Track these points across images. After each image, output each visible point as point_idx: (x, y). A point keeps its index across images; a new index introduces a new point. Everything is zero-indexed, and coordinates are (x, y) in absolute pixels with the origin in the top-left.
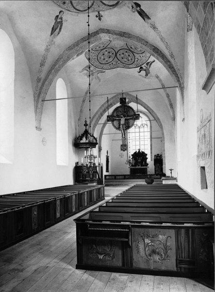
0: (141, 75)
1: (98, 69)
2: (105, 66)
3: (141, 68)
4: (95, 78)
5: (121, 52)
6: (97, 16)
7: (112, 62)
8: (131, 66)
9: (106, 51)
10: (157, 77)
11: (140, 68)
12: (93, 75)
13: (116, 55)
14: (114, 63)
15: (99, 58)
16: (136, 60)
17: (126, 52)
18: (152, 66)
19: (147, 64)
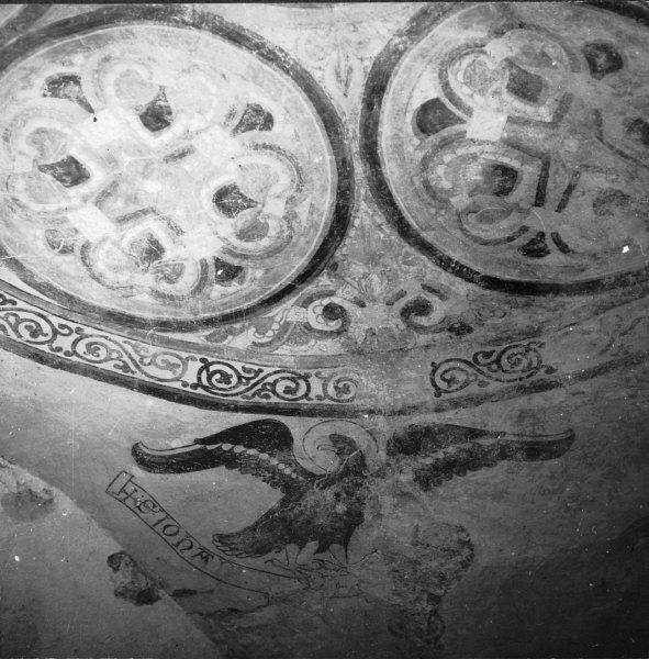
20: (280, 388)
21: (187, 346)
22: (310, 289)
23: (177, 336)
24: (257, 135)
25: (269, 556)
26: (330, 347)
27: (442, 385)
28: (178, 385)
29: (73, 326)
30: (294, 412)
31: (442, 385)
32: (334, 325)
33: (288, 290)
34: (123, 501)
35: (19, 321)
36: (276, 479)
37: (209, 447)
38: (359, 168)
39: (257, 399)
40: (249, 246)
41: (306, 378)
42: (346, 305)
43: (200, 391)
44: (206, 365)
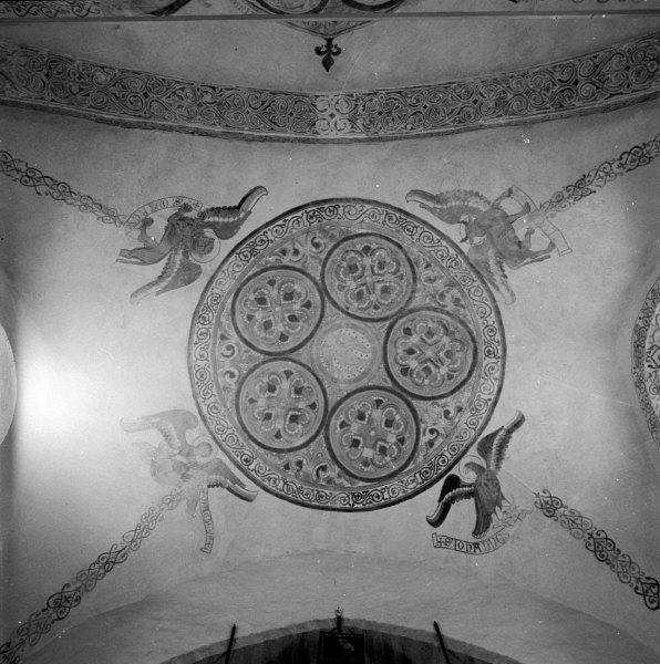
3: (453, 482)
4: (191, 506)
5: (355, 404)
6: (318, 51)
7: (300, 455)
8: (396, 488)
9: (288, 374)
10: (550, 507)
11: (445, 490)
13: (325, 424)
14: (309, 469)
15: (243, 399)
16: (424, 439)
17: (379, 402)
18: (508, 452)
19: (484, 449)
24: (381, 406)
26: (441, 440)
30: (451, 468)
32: (435, 434)
36: (468, 495)
40: (401, 430)
41: (443, 454)
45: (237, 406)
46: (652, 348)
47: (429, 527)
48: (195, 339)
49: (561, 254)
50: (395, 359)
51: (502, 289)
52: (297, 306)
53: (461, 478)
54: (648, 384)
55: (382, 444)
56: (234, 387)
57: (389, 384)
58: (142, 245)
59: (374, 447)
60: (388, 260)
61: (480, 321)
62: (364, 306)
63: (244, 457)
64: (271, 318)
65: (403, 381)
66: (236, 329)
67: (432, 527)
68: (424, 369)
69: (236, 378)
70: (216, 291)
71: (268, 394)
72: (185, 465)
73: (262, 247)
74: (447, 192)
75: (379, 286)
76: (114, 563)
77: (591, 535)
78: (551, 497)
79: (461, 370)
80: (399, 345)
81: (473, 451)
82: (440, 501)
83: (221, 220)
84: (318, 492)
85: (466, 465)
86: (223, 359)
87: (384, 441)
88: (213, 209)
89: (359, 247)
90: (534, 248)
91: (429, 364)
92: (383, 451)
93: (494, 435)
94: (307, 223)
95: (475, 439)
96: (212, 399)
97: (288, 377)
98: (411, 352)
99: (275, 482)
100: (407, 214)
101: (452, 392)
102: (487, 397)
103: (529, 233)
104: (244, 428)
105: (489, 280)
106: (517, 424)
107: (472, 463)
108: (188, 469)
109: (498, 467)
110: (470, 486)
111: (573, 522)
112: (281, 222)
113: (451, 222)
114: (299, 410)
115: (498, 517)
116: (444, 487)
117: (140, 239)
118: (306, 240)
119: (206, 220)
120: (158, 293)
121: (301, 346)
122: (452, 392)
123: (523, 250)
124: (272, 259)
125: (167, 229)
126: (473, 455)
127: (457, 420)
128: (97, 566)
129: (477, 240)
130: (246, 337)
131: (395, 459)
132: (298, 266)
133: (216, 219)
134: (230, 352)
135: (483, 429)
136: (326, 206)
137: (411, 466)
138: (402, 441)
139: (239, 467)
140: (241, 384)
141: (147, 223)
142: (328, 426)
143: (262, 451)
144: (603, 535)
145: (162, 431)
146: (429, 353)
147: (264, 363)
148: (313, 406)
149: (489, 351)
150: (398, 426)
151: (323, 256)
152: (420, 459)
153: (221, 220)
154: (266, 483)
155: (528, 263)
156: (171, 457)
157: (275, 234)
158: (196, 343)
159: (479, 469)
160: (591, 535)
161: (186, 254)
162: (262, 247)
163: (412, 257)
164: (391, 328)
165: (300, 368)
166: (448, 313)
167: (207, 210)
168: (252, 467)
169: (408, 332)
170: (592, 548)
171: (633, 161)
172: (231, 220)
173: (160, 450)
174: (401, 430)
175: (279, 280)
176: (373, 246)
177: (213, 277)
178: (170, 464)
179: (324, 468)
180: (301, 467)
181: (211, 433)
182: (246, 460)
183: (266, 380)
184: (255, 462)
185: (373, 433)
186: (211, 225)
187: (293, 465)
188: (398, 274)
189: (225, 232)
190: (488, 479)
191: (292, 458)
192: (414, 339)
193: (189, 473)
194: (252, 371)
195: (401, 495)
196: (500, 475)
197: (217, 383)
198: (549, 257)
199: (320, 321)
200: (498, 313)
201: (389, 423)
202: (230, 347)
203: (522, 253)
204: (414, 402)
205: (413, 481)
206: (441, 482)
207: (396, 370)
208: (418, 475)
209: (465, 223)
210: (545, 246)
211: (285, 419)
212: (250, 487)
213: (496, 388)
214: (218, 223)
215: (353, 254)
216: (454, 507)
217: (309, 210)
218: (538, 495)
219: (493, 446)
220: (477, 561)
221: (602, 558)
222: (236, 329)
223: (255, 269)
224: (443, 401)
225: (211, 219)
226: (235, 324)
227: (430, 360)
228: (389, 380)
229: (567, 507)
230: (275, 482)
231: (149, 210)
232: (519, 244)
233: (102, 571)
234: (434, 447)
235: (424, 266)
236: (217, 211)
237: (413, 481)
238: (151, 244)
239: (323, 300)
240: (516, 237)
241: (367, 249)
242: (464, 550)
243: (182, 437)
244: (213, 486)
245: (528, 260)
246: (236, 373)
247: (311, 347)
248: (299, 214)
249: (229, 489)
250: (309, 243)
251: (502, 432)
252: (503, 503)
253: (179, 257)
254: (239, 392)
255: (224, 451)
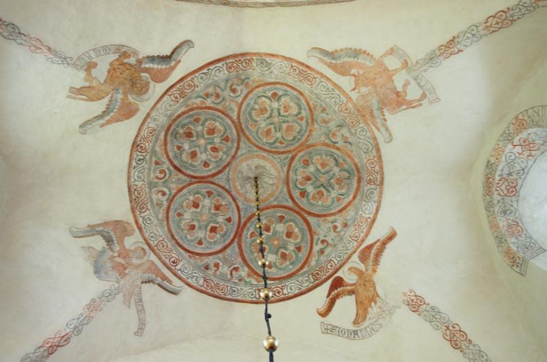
0: (330, 330)
1: (153, 257)
2: (185, 265)
3: (338, 283)
8: (292, 286)
10: (416, 304)
12: (122, 275)
13: (238, 234)
14: (225, 269)
16: (317, 248)
17: (282, 218)
19: (364, 257)
20: (329, 267)
21: (305, 272)
22: (315, 241)
23: (302, 272)
24: (284, 220)
25: (368, 317)
27: (356, 239)
28: (312, 284)
29: (283, 285)
31: (356, 239)
32: (325, 244)
33: (312, 244)
34: (327, 333)
35: (274, 292)
36: (351, 292)
37: (331, 297)
38: (297, 209)
39: (328, 274)
40: (298, 241)
42: (324, 239)
43: (316, 282)
44: (312, 274)
45: (167, 218)
46: (500, 180)
47: (321, 319)
48: (134, 164)
49: (431, 103)
50: (296, 185)
51: (382, 129)
52: (217, 140)
53: (345, 279)
54: (497, 209)
55: (283, 251)
56: (165, 204)
57: (290, 204)
58: (87, 84)
59: (276, 253)
60: (292, 104)
61: (363, 155)
62: (271, 141)
63: (172, 260)
64: (197, 149)
65: (303, 203)
66: (168, 156)
67: (320, 317)
68: (318, 193)
69: (166, 197)
70: (151, 125)
71: (193, 209)
72: (123, 265)
73: (189, 91)
74: (341, 50)
75: (284, 126)
76: (58, 346)
77: (448, 328)
78: (416, 296)
79: (347, 194)
80: (298, 172)
81: (355, 258)
82: (328, 296)
83: (156, 66)
84: (232, 287)
85: (350, 269)
86: (156, 180)
87: (286, 249)
88: (148, 57)
89: (269, 94)
90: (408, 98)
91: (322, 189)
92: (284, 256)
93: (370, 247)
94: (226, 72)
95: (358, 247)
96: (147, 213)
97: (209, 196)
98: (308, 179)
99: (197, 280)
100: (308, 67)
101: (340, 211)
102: (367, 216)
103: (406, 84)
104: (172, 236)
105: (372, 123)
106: (391, 237)
107: (356, 268)
108: (125, 269)
109: (374, 271)
110: (352, 285)
111: (433, 315)
112: (205, 71)
113: (343, 74)
114: (218, 223)
115: (373, 311)
116: (332, 286)
117: (86, 80)
118: (225, 87)
119: (143, 66)
120: (102, 126)
121: (220, 172)
122: (340, 211)
123: (400, 99)
124: (198, 101)
125: (109, 72)
126: (355, 261)
127: (343, 233)
128: (42, 349)
129: (364, 90)
130: (176, 163)
131: (292, 264)
132: (219, 107)
133: (151, 65)
134: (163, 175)
135: (363, 241)
136: (242, 59)
137: (305, 269)
138: (299, 249)
139: (168, 268)
140: (171, 201)
141: (91, 66)
142: (241, 236)
143: (186, 255)
144: (457, 328)
145: (104, 237)
146: (323, 180)
147: (190, 184)
148: (229, 220)
149: (370, 179)
150: (297, 237)
151: (239, 100)
152: (313, 263)
153: (156, 66)
154: (190, 281)
155: (404, 110)
156: (112, 258)
157: (200, 80)
158: (135, 168)
159: (360, 274)
160: (448, 328)
161: (125, 94)
162: (189, 91)
163: (311, 103)
164: (293, 159)
165: (220, 190)
166: (338, 149)
167: (144, 58)
168: (178, 267)
169: (306, 163)
170: (448, 338)
171: (497, 23)
172: (164, 67)
173: (103, 252)
174: (298, 241)
175: (202, 118)
176: (280, 93)
177: (148, 115)
178: (109, 264)
179: (236, 269)
180: (218, 268)
181: (145, 240)
182: (174, 262)
183: (191, 198)
184: (181, 264)
185: (276, 242)
186: (146, 70)
187: (212, 266)
188: (300, 116)
189: (159, 77)
190: (366, 280)
191: (211, 260)
192: (312, 169)
193: (127, 271)
194: (180, 190)
195: (297, 291)
196: (376, 278)
197: (152, 201)
198: (421, 105)
199: (236, 153)
200: (378, 150)
201: (289, 235)
202: (162, 172)
203: (398, 101)
204: (310, 219)
205: (307, 280)
206: (329, 283)
207: (296, 194)
208: (311, 276)
209: (354, 75)
210: (418, 97)
211: (206, 230)
212: (177, 283)
213: (375, 208)
214: (153, 68)
215: (264, 99)
216: (338, 302)
217: (228, 62)
218: (404, 294)
219: (372, 254)
220: (355, 346)
221: (456, 346)
222: (168, 156)
223: (183, 109)
224: (333, 218)
225: (147, 66)
226: (167, 153)
227: (322, 185)
228: (290, 200)
229: (428, 304)
230: (197, 280)
231: (93, 54)
232: (398, 94)
233: (46, 353)
234: (325, 254)
235: (320, 110)
236: (152, 59)
237: (307, 280)
238: (95, 84)
239: (238, 135)
240: (395, 88)
241: (275, 95)
242: (346, 335)
243: (121, 242)
244: (146, 282)
245: (404, 107)
246: (166, 190)
247: (229, 173)
248: (220, 64)
249: (160, 285)
250: (228, 88)
251: (378, 243)
252: (378, 299)
253: (120, 96)
254: (169, 208)
255: (156, 254)
